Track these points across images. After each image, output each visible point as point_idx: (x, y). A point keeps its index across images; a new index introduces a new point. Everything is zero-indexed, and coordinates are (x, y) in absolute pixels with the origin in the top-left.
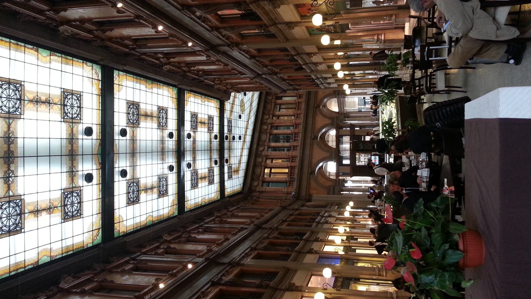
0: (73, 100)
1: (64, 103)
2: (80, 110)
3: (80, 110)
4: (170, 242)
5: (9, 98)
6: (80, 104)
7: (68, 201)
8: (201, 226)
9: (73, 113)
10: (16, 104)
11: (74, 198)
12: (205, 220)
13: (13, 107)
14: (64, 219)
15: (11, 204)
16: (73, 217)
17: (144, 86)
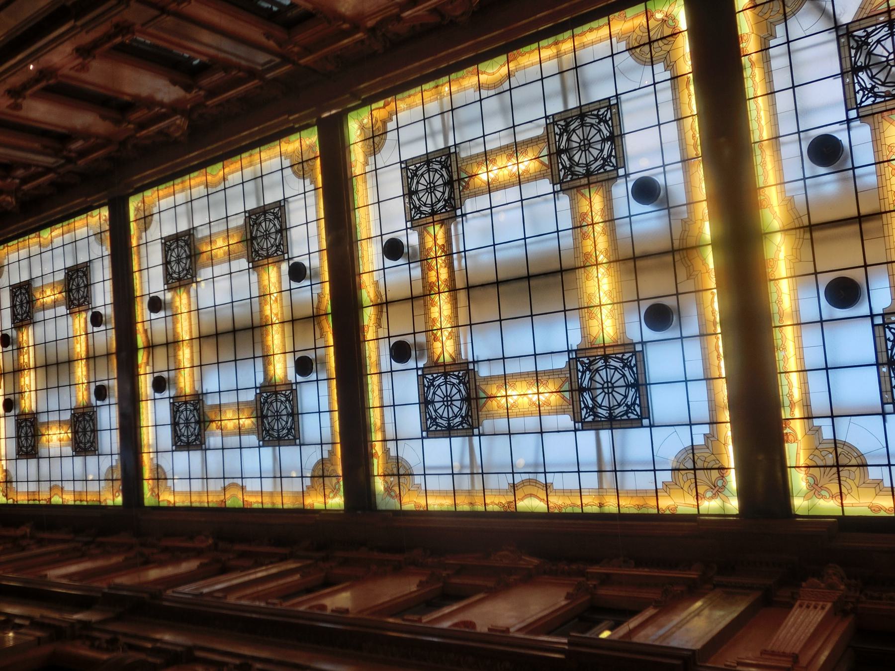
0: (445, 415)
1: (469, 405)
2: (426, 398)
3: (426, 398)
4: (174, 108)
5: (608, 388)
6: (427, 407)
7: (444, 193)
8: (69, 160)
9: (443, 388)
10: (591, 379)
11: (429, 202)
12: (52, 183)
13: (597, 371)
14: (449, 155)
15: (582, 170)
16: (427, 160)
17: (248, 489)
